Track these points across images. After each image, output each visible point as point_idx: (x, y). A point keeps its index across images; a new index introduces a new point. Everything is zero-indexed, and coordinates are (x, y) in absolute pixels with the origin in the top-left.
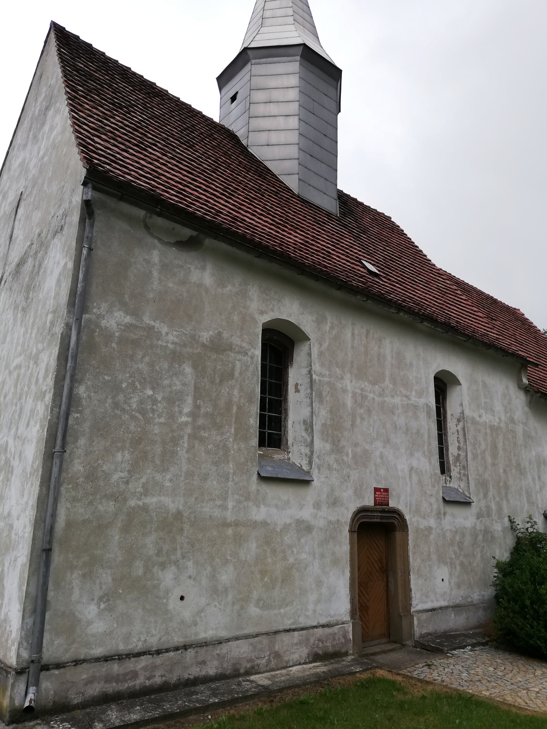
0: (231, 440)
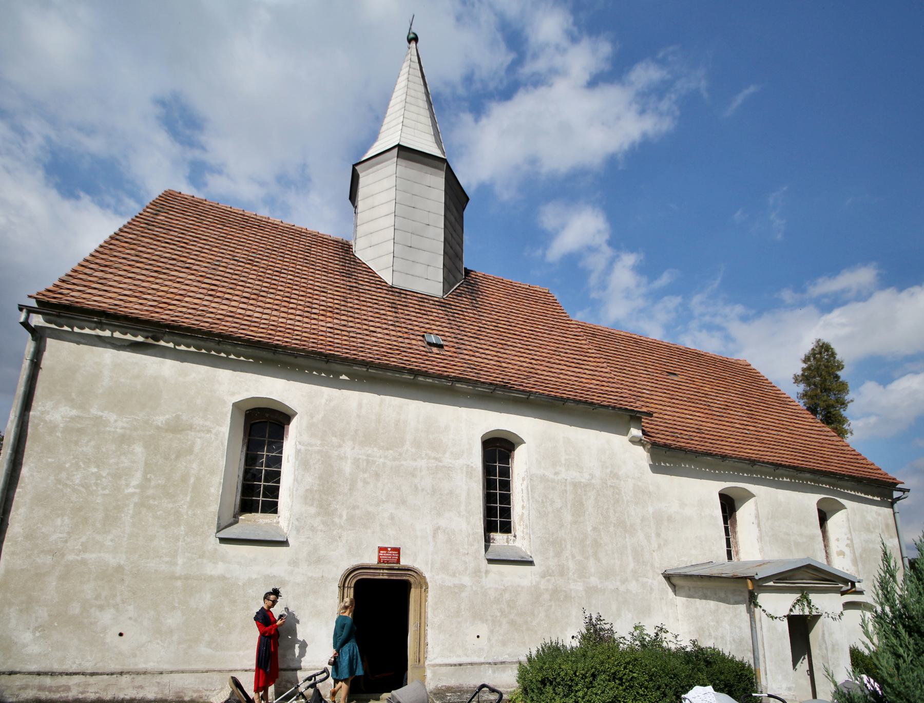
0: (185, 507)
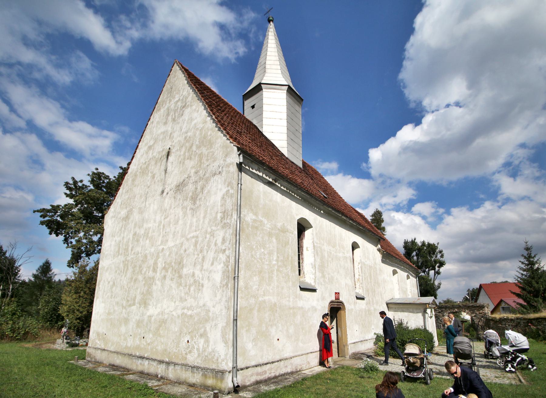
0: (290, 272)
